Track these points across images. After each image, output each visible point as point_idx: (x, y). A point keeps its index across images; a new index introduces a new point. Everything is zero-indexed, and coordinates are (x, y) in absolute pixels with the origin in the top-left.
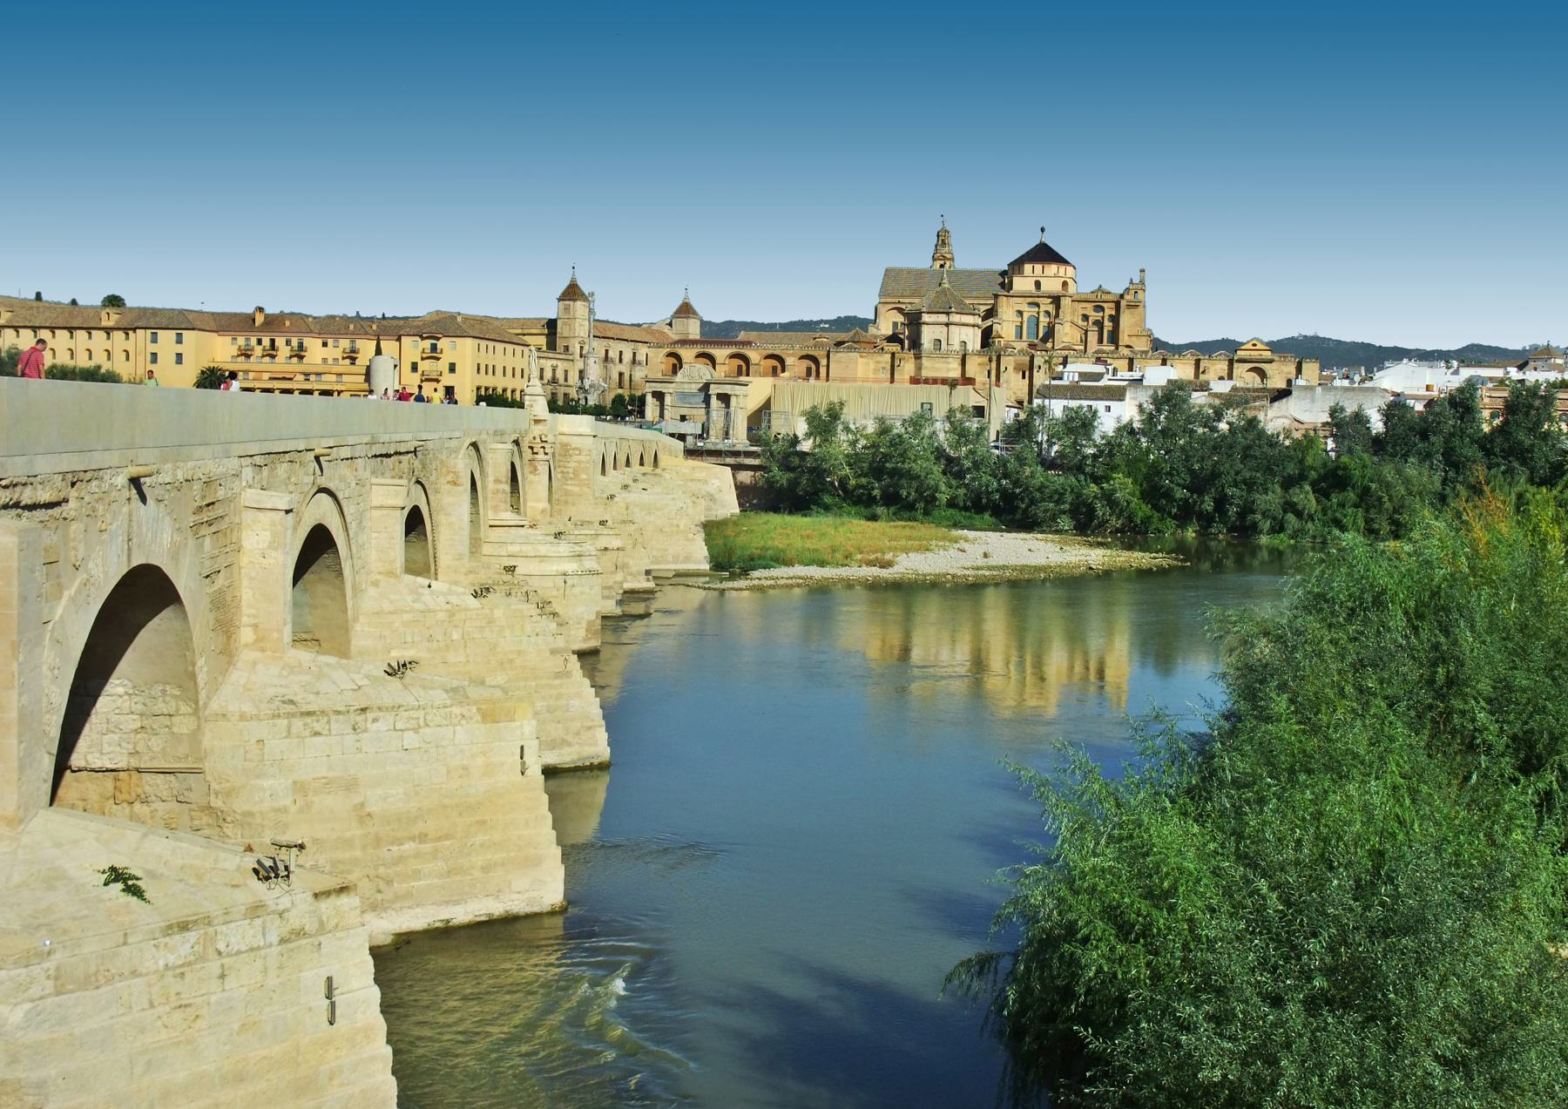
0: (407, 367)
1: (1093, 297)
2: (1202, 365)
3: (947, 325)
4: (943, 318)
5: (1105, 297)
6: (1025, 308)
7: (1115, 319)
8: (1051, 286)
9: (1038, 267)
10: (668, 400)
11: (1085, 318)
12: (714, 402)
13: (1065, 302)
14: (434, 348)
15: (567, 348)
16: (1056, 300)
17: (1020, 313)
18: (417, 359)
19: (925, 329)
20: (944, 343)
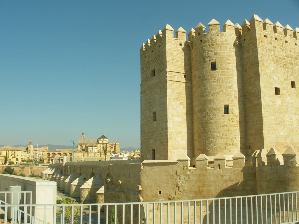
0: (10, 155)
1: (111, 143)
2: (131, 154)
3: (92, 148)
4: (92, 147)
5: (113, 143)
6: (101, 145)
7: (115, 147)
8: (105, 142)
9: (103, 139)
10: (53, 160)
11: (110, 147)
12: (61, 160)
13: (108, 144)
14: (15, 152)
15: (30, 152)
16: (106, 144)
17: (101, 146)
18: (12, 154)
19: (89, 149)
20: (92, 151)
